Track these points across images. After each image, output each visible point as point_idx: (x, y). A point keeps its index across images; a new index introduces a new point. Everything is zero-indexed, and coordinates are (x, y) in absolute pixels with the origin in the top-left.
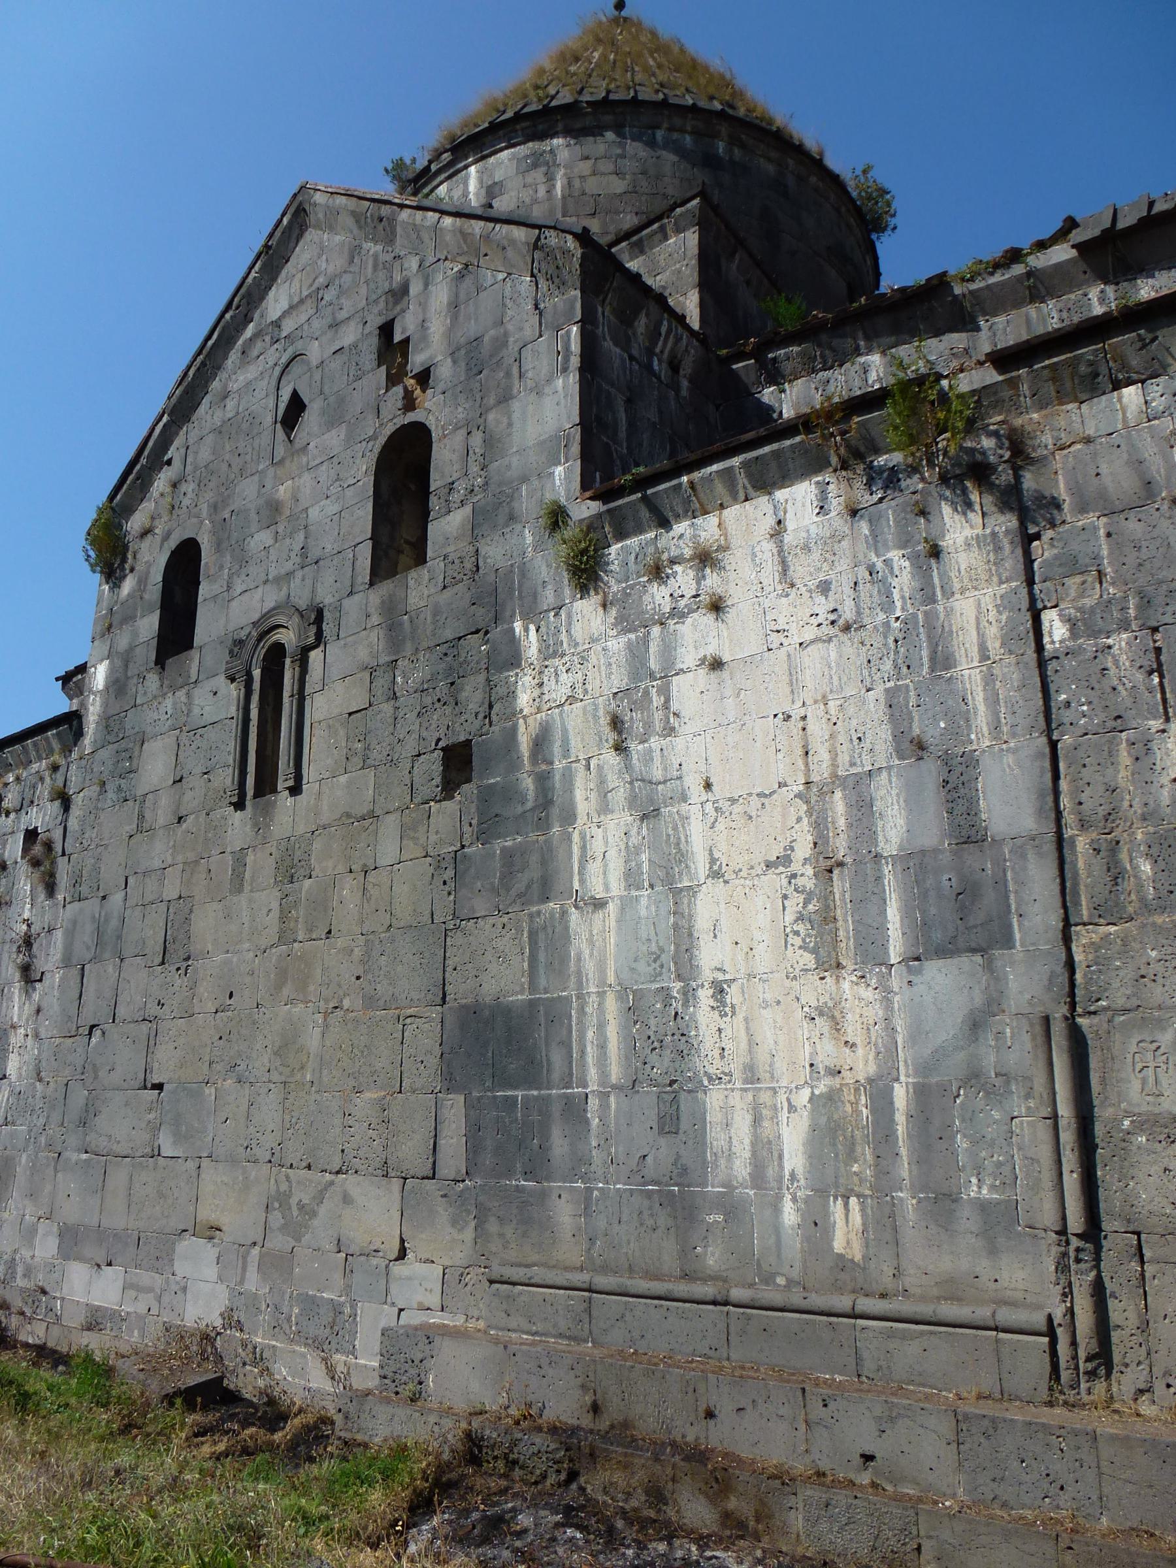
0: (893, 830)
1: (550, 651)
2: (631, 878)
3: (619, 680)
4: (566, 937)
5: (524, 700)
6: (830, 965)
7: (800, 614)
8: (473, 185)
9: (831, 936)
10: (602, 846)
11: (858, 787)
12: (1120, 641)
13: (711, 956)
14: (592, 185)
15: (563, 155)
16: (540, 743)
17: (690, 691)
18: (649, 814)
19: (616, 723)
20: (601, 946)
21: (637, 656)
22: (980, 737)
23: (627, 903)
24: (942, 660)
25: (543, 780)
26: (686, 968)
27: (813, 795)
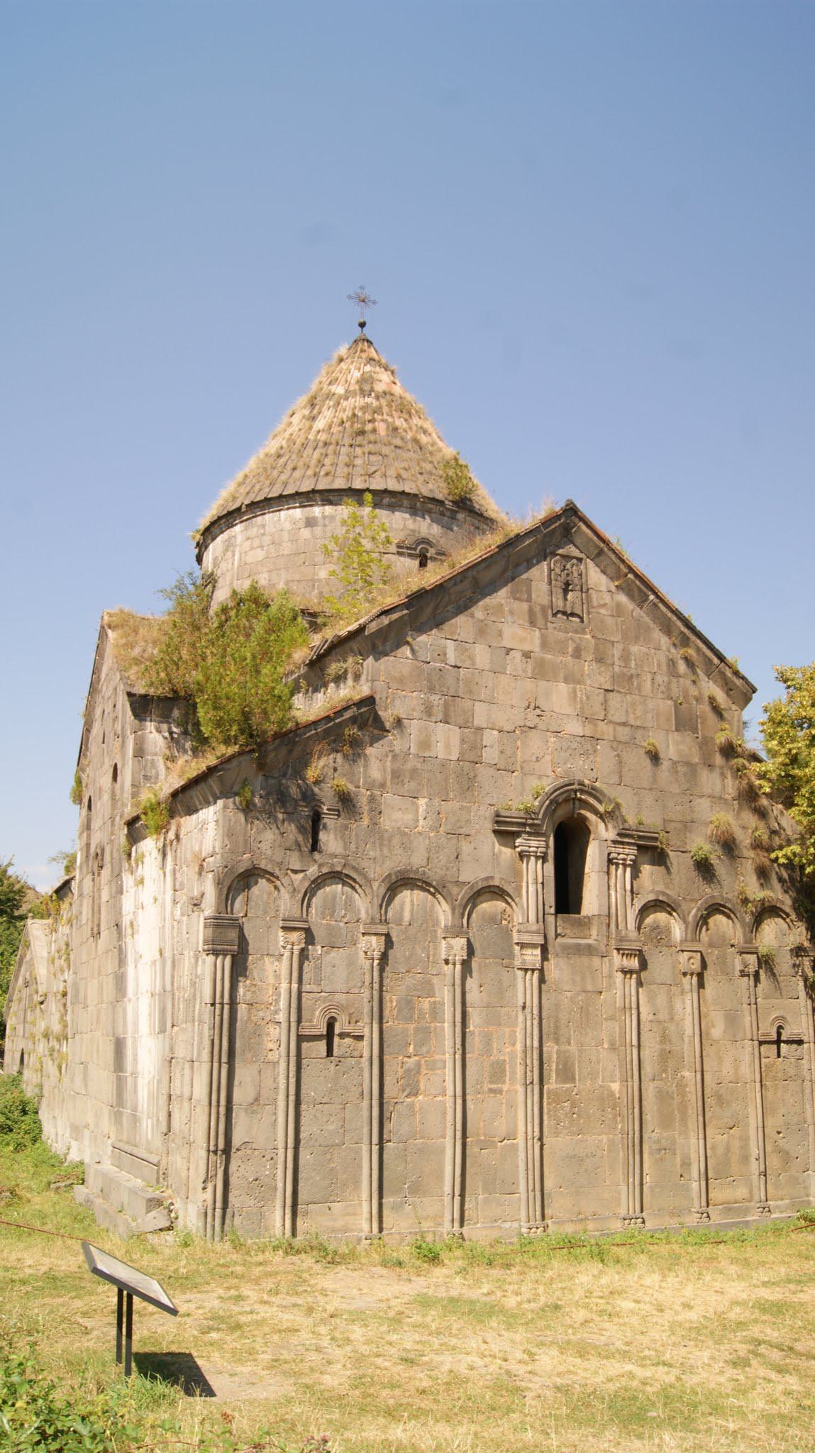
12: (185, 918)
14: (249, 559)
15: (239, 539)
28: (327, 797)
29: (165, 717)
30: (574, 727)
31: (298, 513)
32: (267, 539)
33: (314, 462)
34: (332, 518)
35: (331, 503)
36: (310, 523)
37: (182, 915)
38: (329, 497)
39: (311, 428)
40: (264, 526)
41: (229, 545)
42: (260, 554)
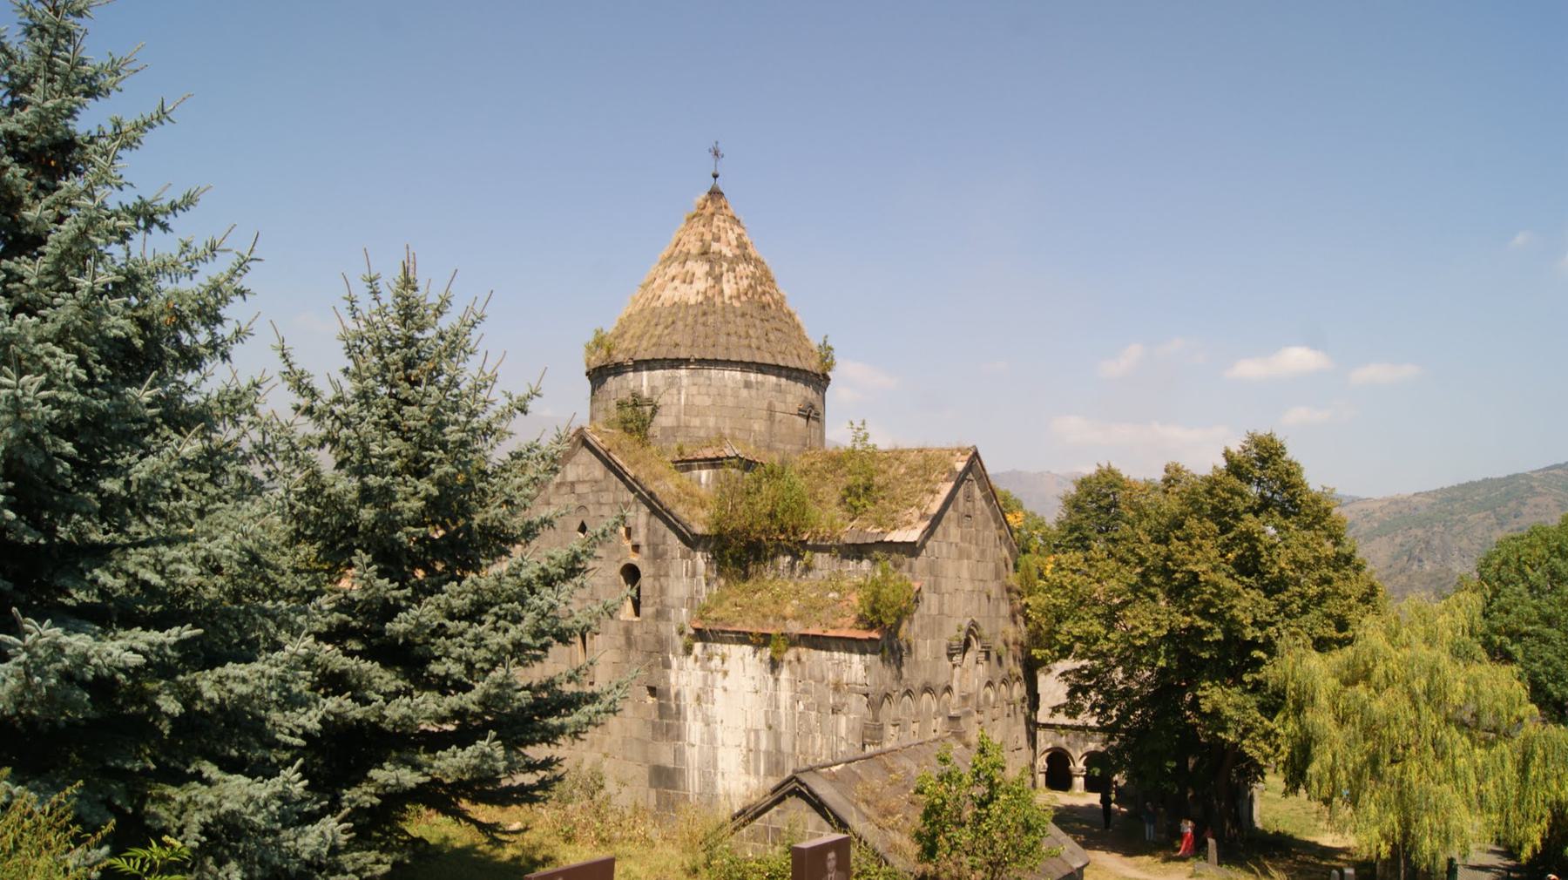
0: (763, 745)
1: (681, 668)
2: (702, 740)
3: (700, 684)
4: (684, 753)
5: (673, 680)
6: (748, 773)
7: (748, 685)
8: (645, 383)
9: (748, 766)
10: (694, 729)
11: (757, 732)
12: (813, 713)
13: (721, 765)
14: (698, 400)
15: (685, 382)
16: (677, 695)
17: (718, 693)
18: (707, 725)
19: (698, 698)
20: (693, 756)
21: (705, 678)
22: (783, 729)
23: (701, 748)
24: (777, 707)
25: (678, 706)
26: (715, 767)
27: (748, 731)
28: (903, 644)
29: (705, 549)
30: (968, 587)
31: (738, 375)
32: (713, 391)
33: (742, 332)
34: (763, 384)
35: (763, 372)
36: (748, 385)
37: (807, 707)
38: (762, 368)
39: (722, 292)
40: (710, 379)
41: (671, 383)
42: (708, 402)
